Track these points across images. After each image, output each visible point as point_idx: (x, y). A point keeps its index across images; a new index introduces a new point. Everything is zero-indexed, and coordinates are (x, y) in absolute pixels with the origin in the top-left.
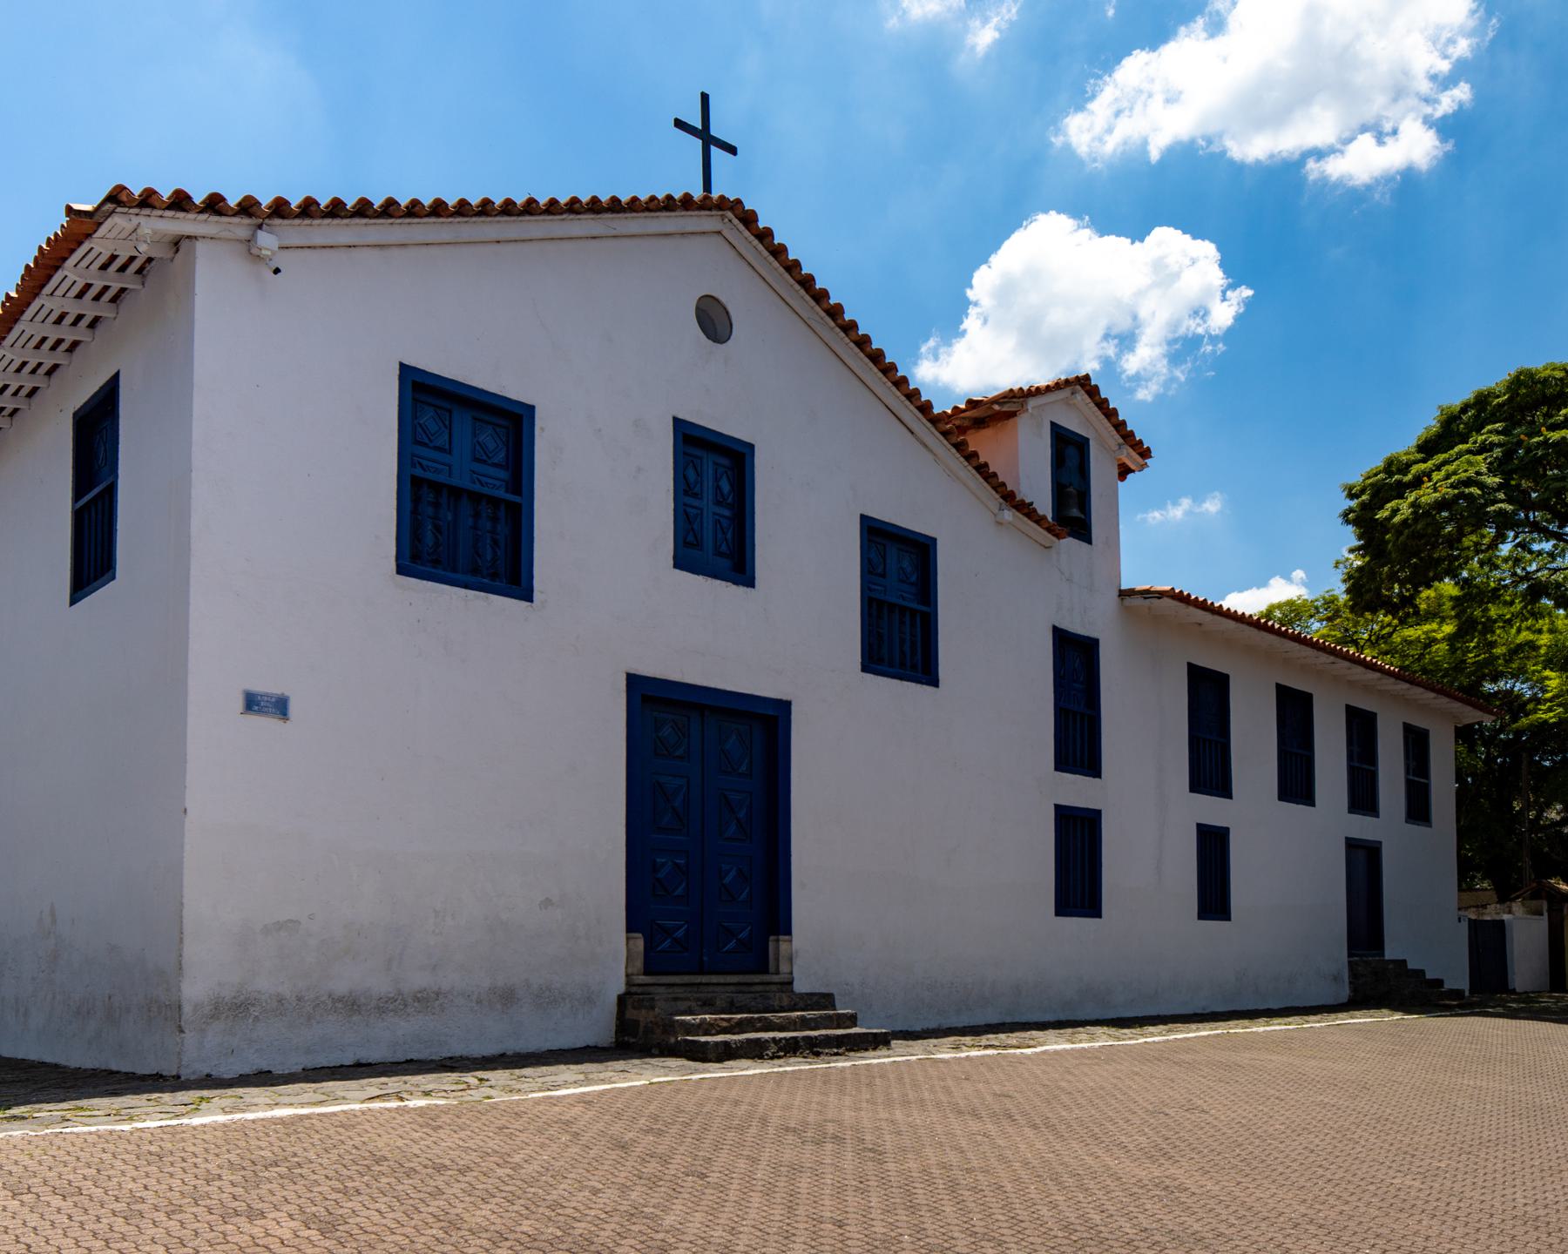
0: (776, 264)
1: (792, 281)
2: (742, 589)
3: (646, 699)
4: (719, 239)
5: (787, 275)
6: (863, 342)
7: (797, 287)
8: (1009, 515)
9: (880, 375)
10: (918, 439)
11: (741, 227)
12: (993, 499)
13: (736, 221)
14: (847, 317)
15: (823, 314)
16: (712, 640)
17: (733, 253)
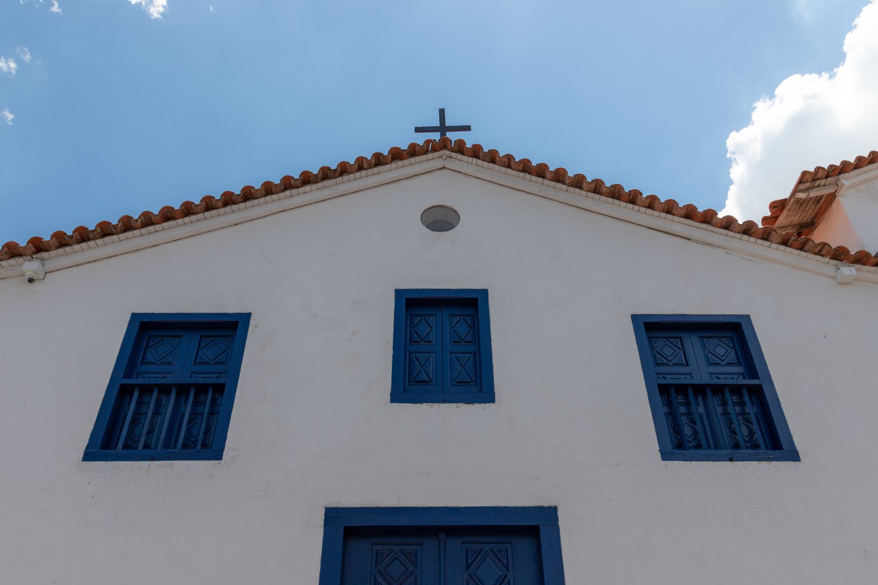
0: (497, 167)
1: (516, 173)
2: (477, 407)
3: (351, 533)
4: (446, 172)
5: (509, 171)
6: (597, 187)
7: (521, 174)
8: (849, 271)
9: (630, 206)
10: (697, 242)
11: (459, 156)
12: (825, 265)
13: (454, 155)
14: (571, 174)
15: (553, 184)
16: (444, 459)
17: (460, 175)
